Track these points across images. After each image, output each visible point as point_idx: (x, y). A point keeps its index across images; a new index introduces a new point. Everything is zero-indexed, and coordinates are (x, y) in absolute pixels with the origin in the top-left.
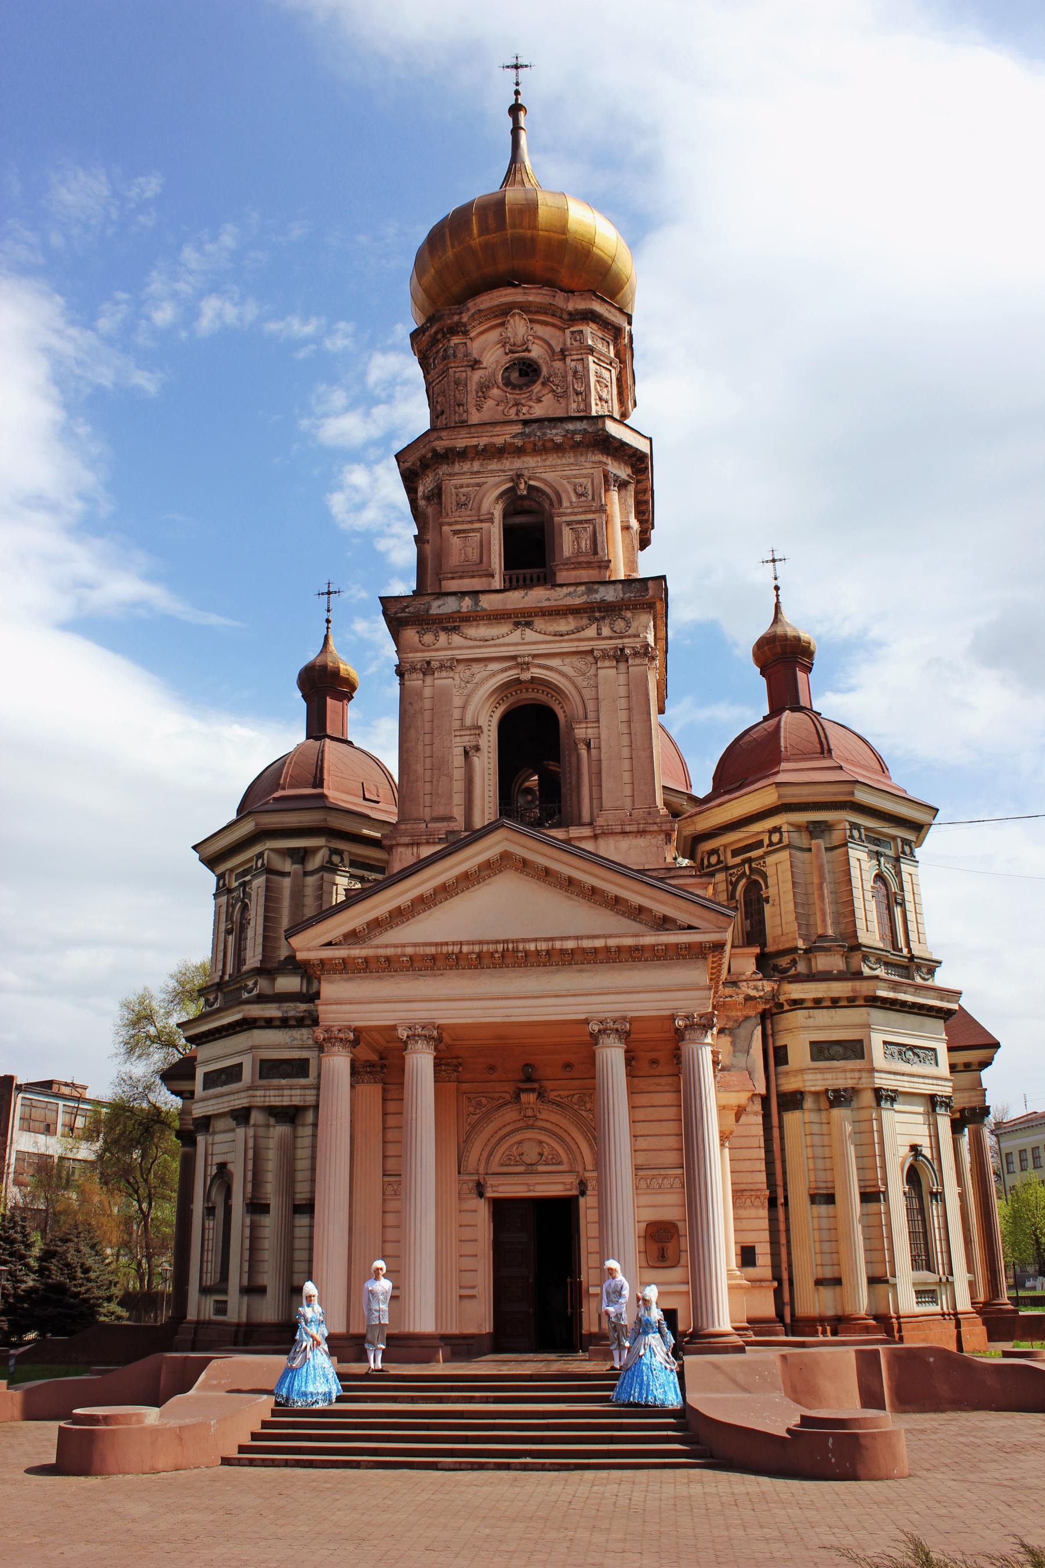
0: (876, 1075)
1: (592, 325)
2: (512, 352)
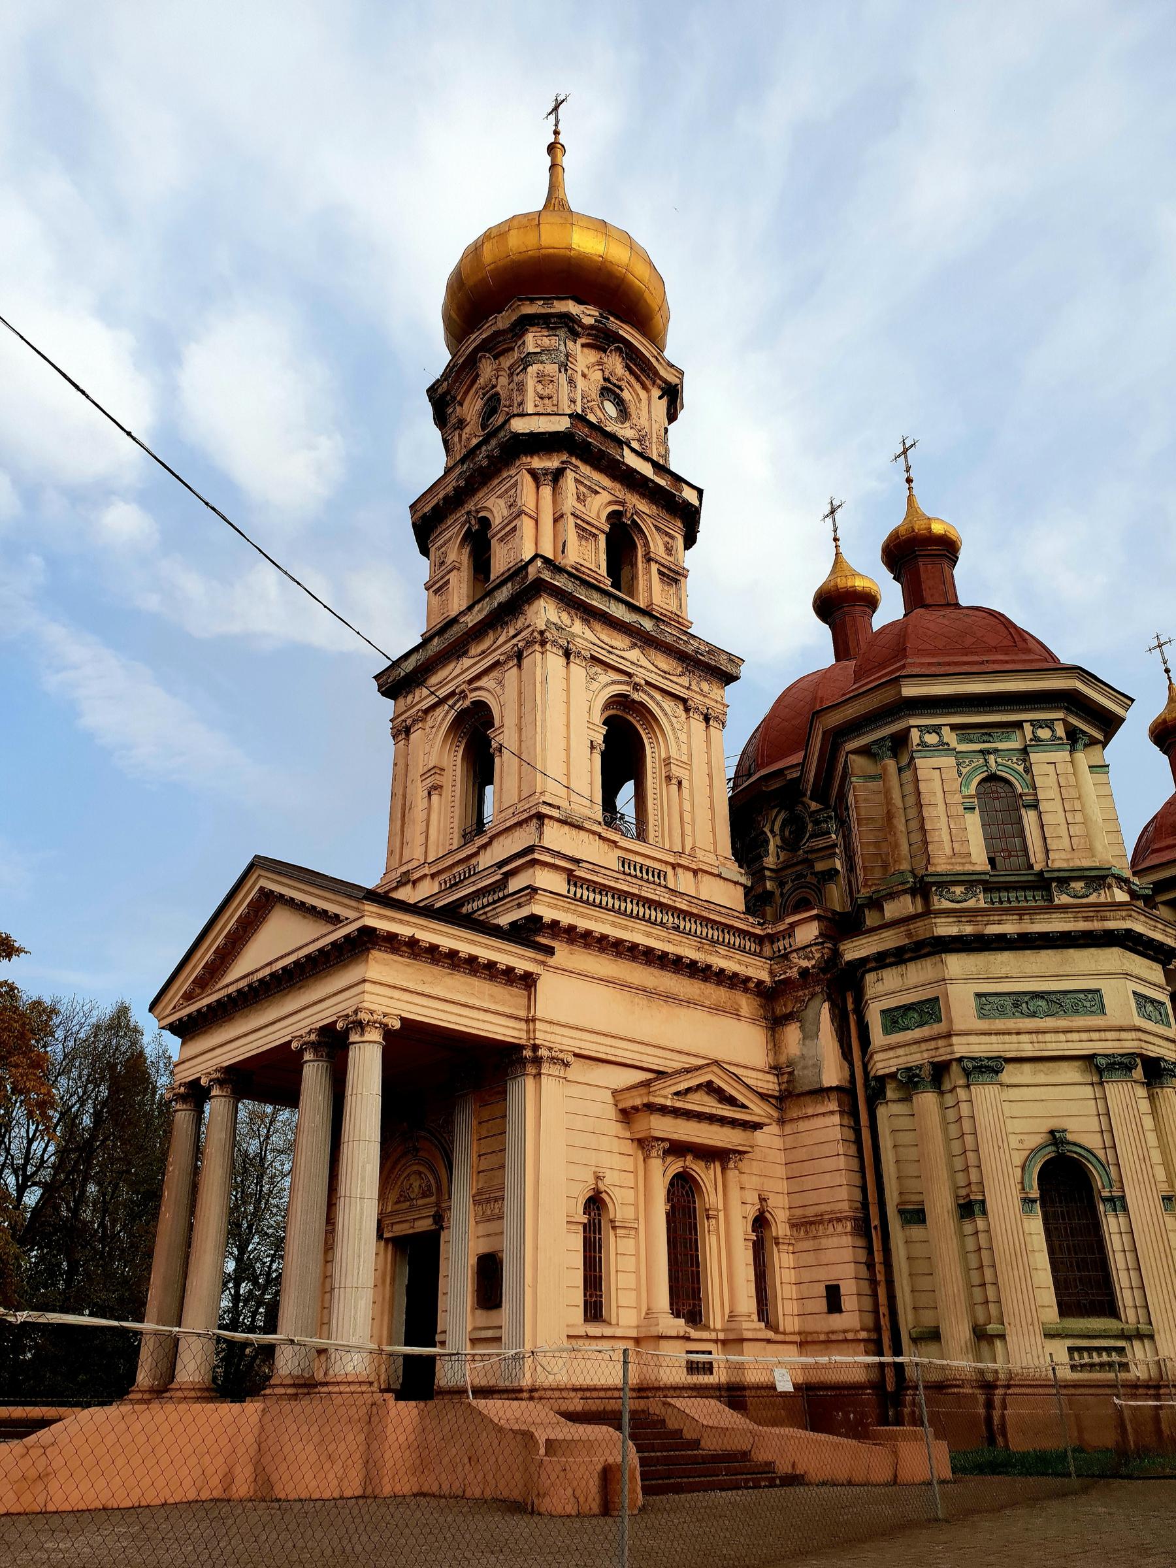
0: (955, 1040)
1: (532, 329)
2: (484, 395)
